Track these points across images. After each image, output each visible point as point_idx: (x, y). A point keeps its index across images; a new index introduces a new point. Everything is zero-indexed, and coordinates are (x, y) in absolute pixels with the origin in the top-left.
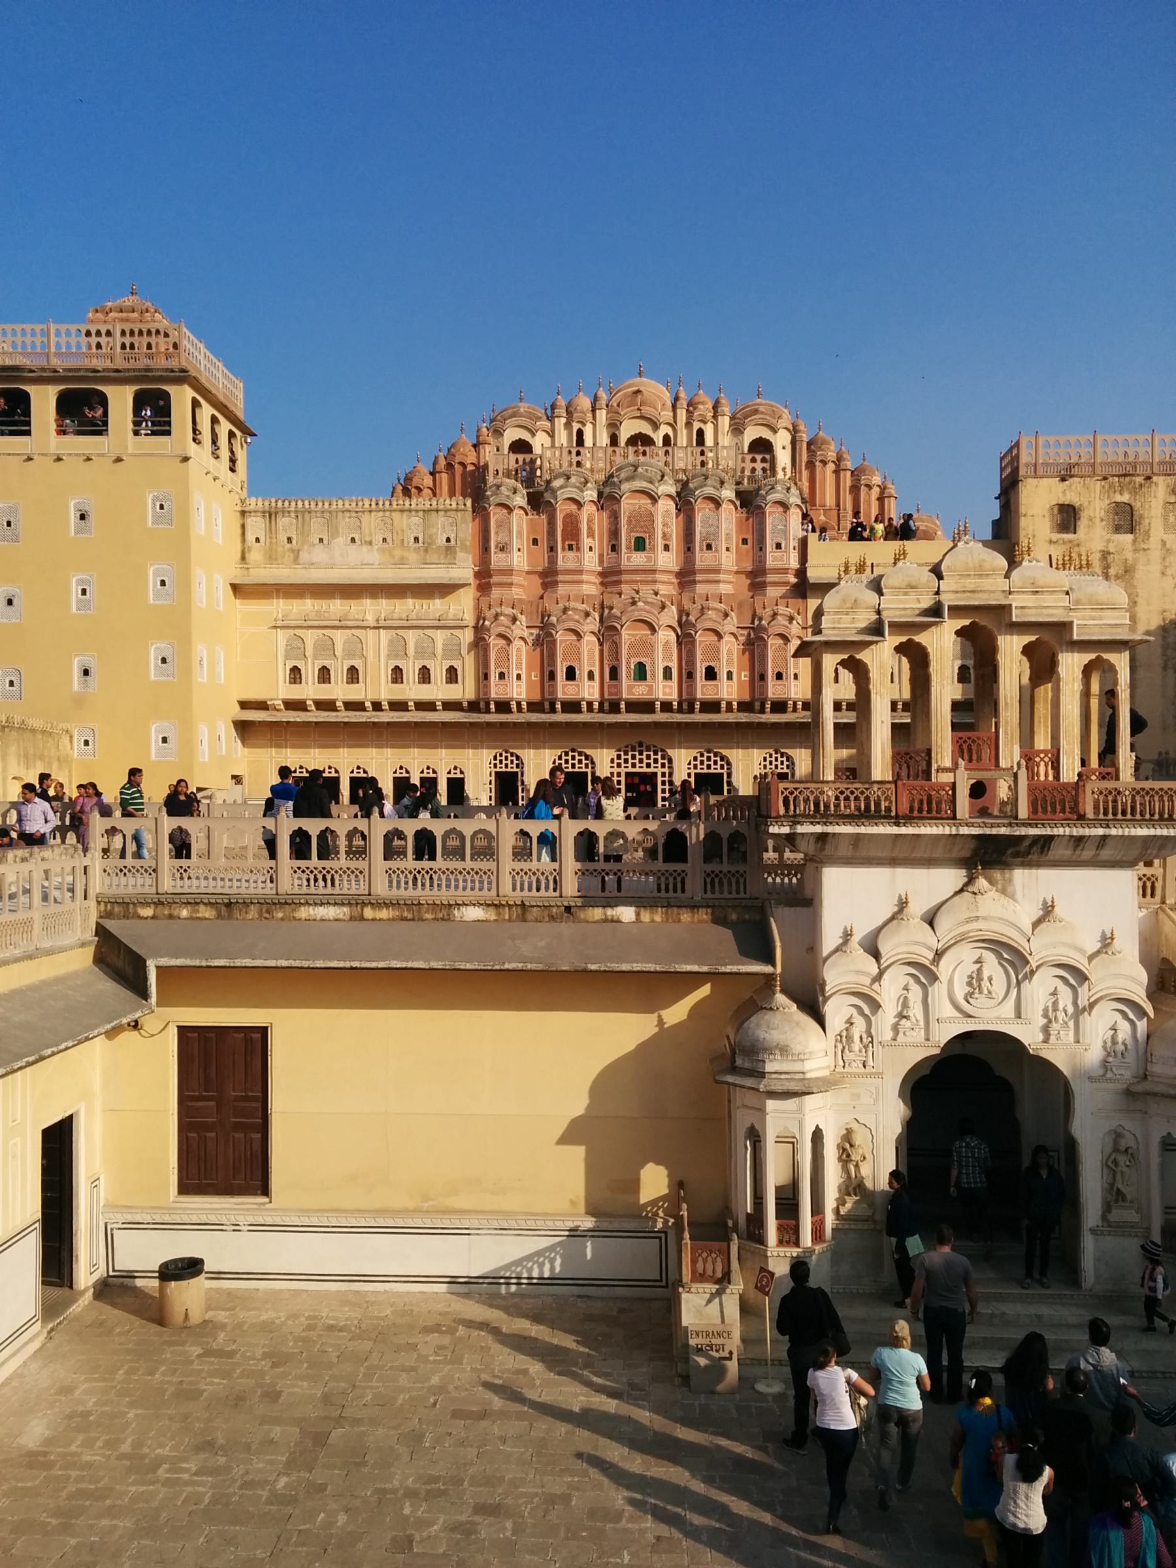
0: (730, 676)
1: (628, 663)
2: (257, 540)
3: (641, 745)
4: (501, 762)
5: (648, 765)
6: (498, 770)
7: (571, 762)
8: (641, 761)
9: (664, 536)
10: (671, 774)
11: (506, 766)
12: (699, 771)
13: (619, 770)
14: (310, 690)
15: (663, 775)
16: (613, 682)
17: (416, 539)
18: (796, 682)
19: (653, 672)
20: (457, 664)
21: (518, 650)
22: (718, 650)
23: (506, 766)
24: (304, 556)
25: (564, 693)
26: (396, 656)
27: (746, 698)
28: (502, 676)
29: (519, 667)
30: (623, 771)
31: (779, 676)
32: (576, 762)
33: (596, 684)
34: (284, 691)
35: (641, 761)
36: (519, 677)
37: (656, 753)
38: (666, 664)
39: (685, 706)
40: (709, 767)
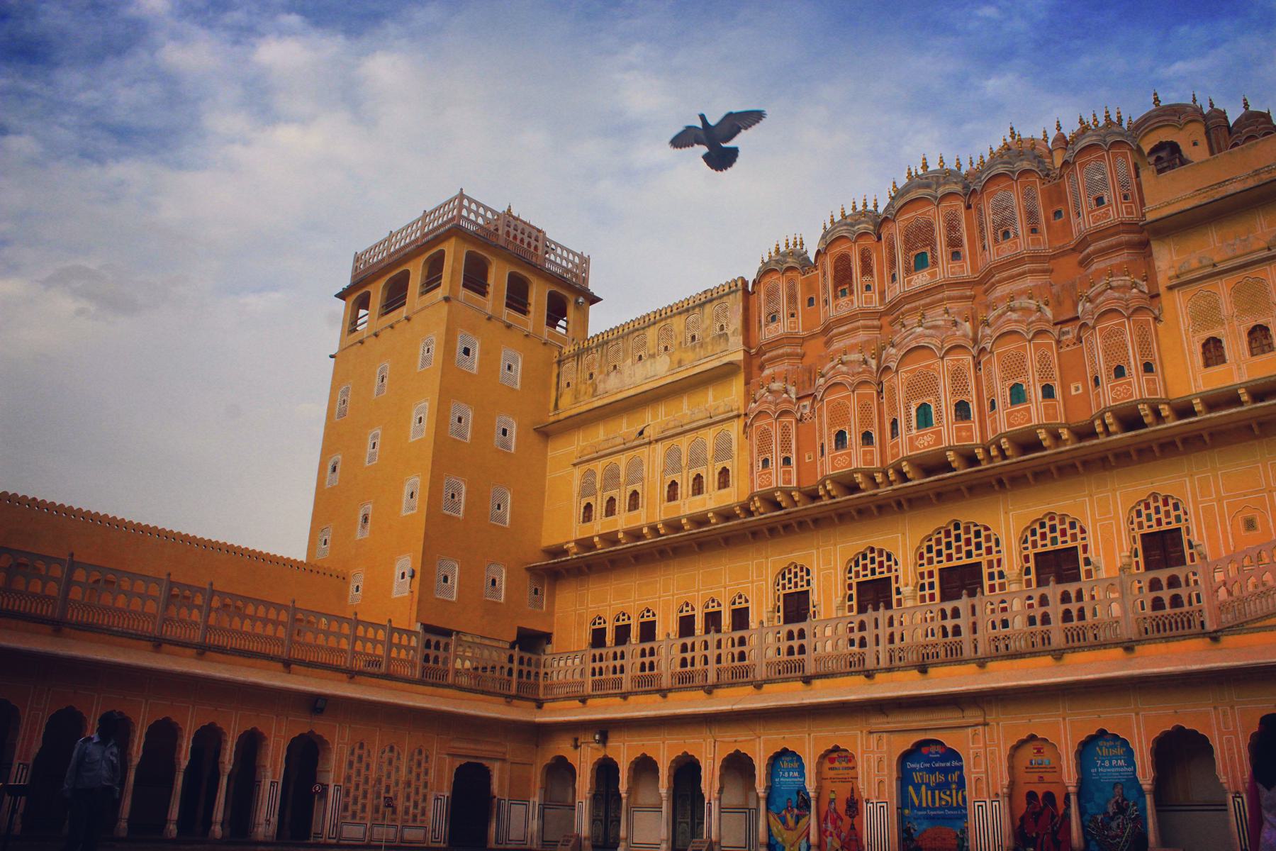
0: (1048, 392)
1: (908, 408)
2: (568, 385)
3: (957, 527)
4: (790, 581)
5: (969, 554)
6: (787, 591)
7: (870, 566)
8: (959, 549)
9: (954, 243)
10: (999, 561)
11: (796, 586)
12: (1040, 550)
13: (931, 568)
14: (600, 525)
15: (990, 564)
16: (895, 441)
17: (693, 338)
18: (1149, 376)
19: (939, 412)
20: (727, 464)
21: (785, 430)
22: (1022, 360)
23: (796, 586)
24: (601, 387)
25: (834, 468)
26: (673, 471)
27: (1081, 418)
28: (766, 462)
29: (785, 445)
30: (935, 568)
31: (1119, 372)
32: (876, 565)
33: (876, 449)
34: (578, 531)
35: (959, 549)
36: (787, 461)
37: (978, 534)
38: (958, 399)
39: (994, 452)
40: (1054, 541)
